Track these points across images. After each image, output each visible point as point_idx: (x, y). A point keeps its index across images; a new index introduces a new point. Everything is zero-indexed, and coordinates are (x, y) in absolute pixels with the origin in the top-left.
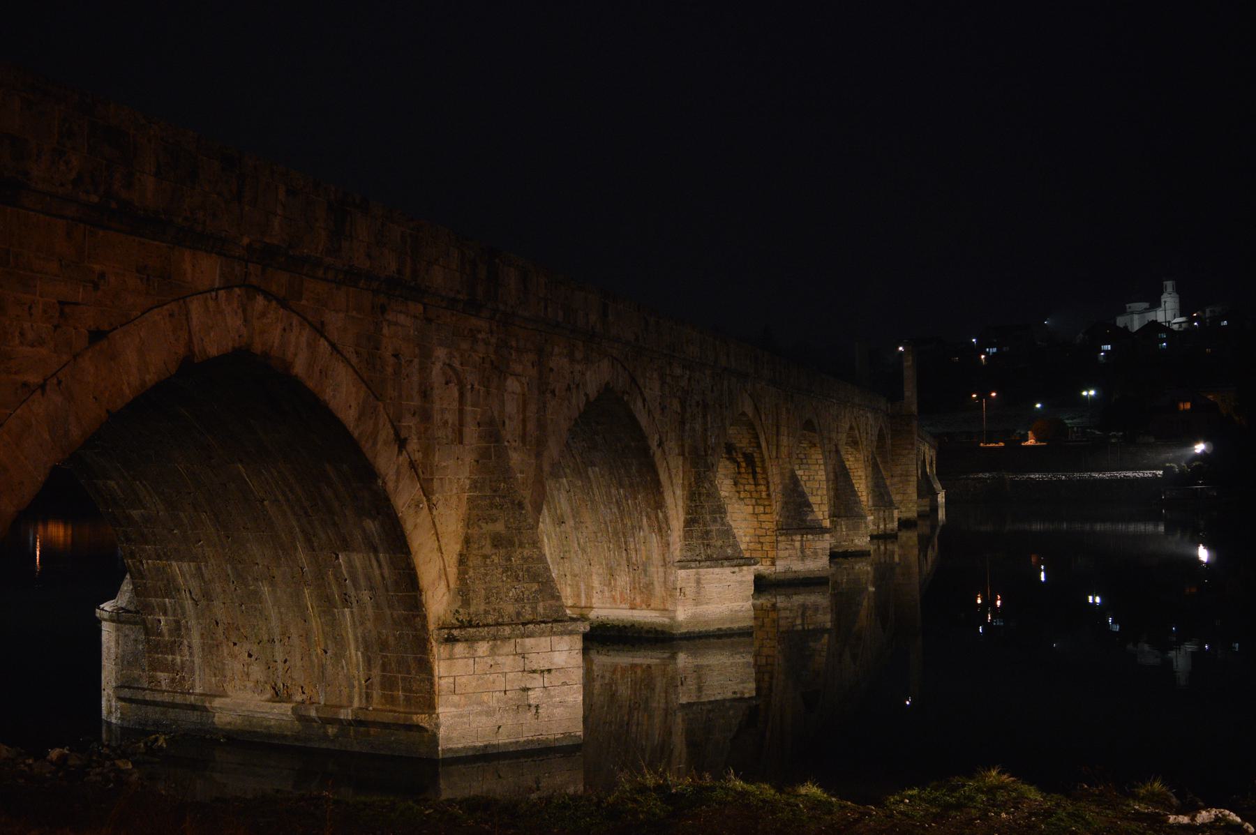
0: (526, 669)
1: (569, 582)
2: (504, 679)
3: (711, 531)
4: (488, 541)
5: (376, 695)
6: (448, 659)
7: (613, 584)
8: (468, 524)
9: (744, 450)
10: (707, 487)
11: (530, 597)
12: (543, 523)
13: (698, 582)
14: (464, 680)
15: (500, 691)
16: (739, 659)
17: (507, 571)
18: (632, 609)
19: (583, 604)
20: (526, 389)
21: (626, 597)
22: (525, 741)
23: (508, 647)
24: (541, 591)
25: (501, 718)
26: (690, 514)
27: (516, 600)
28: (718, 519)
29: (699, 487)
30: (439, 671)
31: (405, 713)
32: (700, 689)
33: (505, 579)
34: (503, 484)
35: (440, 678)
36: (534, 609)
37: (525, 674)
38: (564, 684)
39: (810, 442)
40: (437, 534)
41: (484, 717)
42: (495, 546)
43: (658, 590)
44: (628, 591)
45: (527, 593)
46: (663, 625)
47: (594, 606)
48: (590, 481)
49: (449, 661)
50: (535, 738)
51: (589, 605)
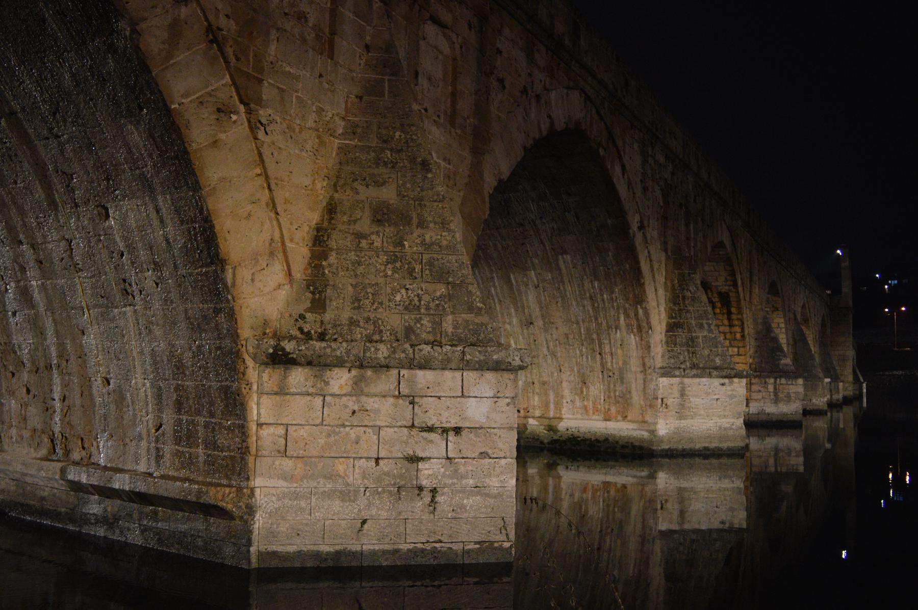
0: (416, 424)
1: (537, 390)
2: (375, 437)
3: (697, 337)
4: (367, 213)
5: (168, 449)
6: (276, 394)
7: (585, 393)
8: (335, 185)
9: (719, 288)
10: (692, 291)
11: (432, 305)
12: (510, 324)
13: (683, 394)
14: (303, 432)
15: (368, 458)
16: (726, 484)
17: (395, 261)
18: (606, 420)
19: (552, 414)
20: (458, 52)
21: (599, 407)
22: (408, 550)
23: (386, 382)
24: (450, 297)
25: (369, 506)
26: (672, 318)
27: (406, 308)
28: (706, 326)
29: (684, 289)
30: (259, 414)
31: (204, 483)
32: (682, 513)
33: (390, 273)
34: (398, 134)
35: (260, 425)
36: (437, 325)
37: (414, 432)
38: (484, 455)
39: (773, 307)
40: (267, 178)
41: (337, 502)
42: (378, 222)
43: (637, 398)
44: (602, 401)
45: (426, 298)
46: (641, 440)
47: (564, 417)
48: (561, 274)
49: (278, 398)
50: (428, 547)
51: (558, 416)
